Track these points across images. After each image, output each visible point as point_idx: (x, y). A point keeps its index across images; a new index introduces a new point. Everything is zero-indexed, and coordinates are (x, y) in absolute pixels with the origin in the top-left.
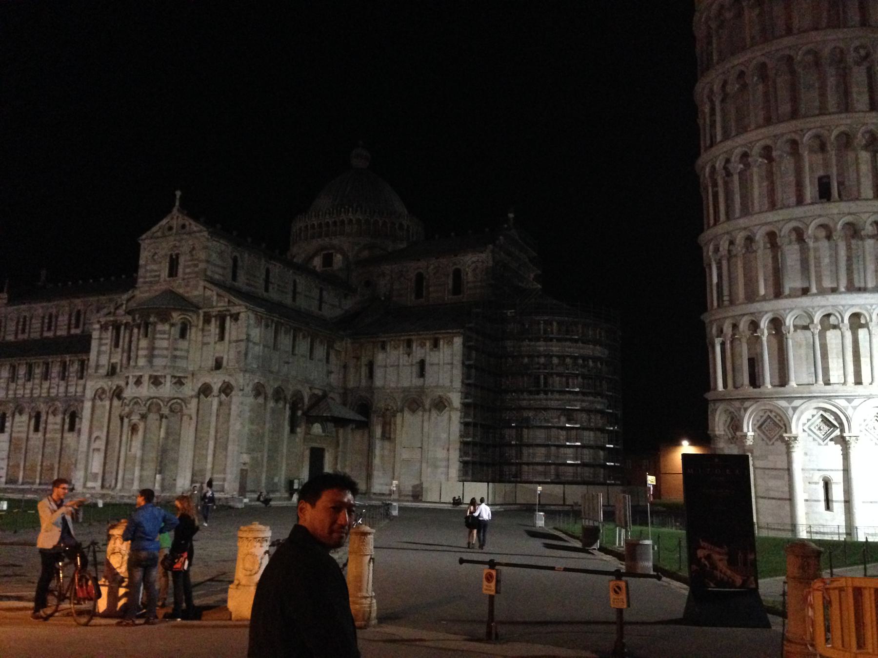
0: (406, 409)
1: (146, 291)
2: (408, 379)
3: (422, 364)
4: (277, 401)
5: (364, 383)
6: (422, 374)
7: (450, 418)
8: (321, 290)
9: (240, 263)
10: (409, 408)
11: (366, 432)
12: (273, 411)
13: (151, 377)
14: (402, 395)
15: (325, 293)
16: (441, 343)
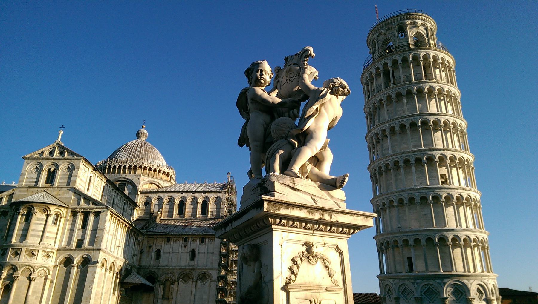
0: (181, 280)
1: (25, 191)
2: (185, 261)
3: (193, 252)
4: (110, 272)
5: (153, 262)
6: (193, 258)
7: (210, 286)
8: (125, 203)
9: (92, 181)
10: (183, 278)
11: (152, 295)
12: (108, 279)
13: (27, 250)
14: (180, 271)
15: (126, 206)
16: (207, 240)
